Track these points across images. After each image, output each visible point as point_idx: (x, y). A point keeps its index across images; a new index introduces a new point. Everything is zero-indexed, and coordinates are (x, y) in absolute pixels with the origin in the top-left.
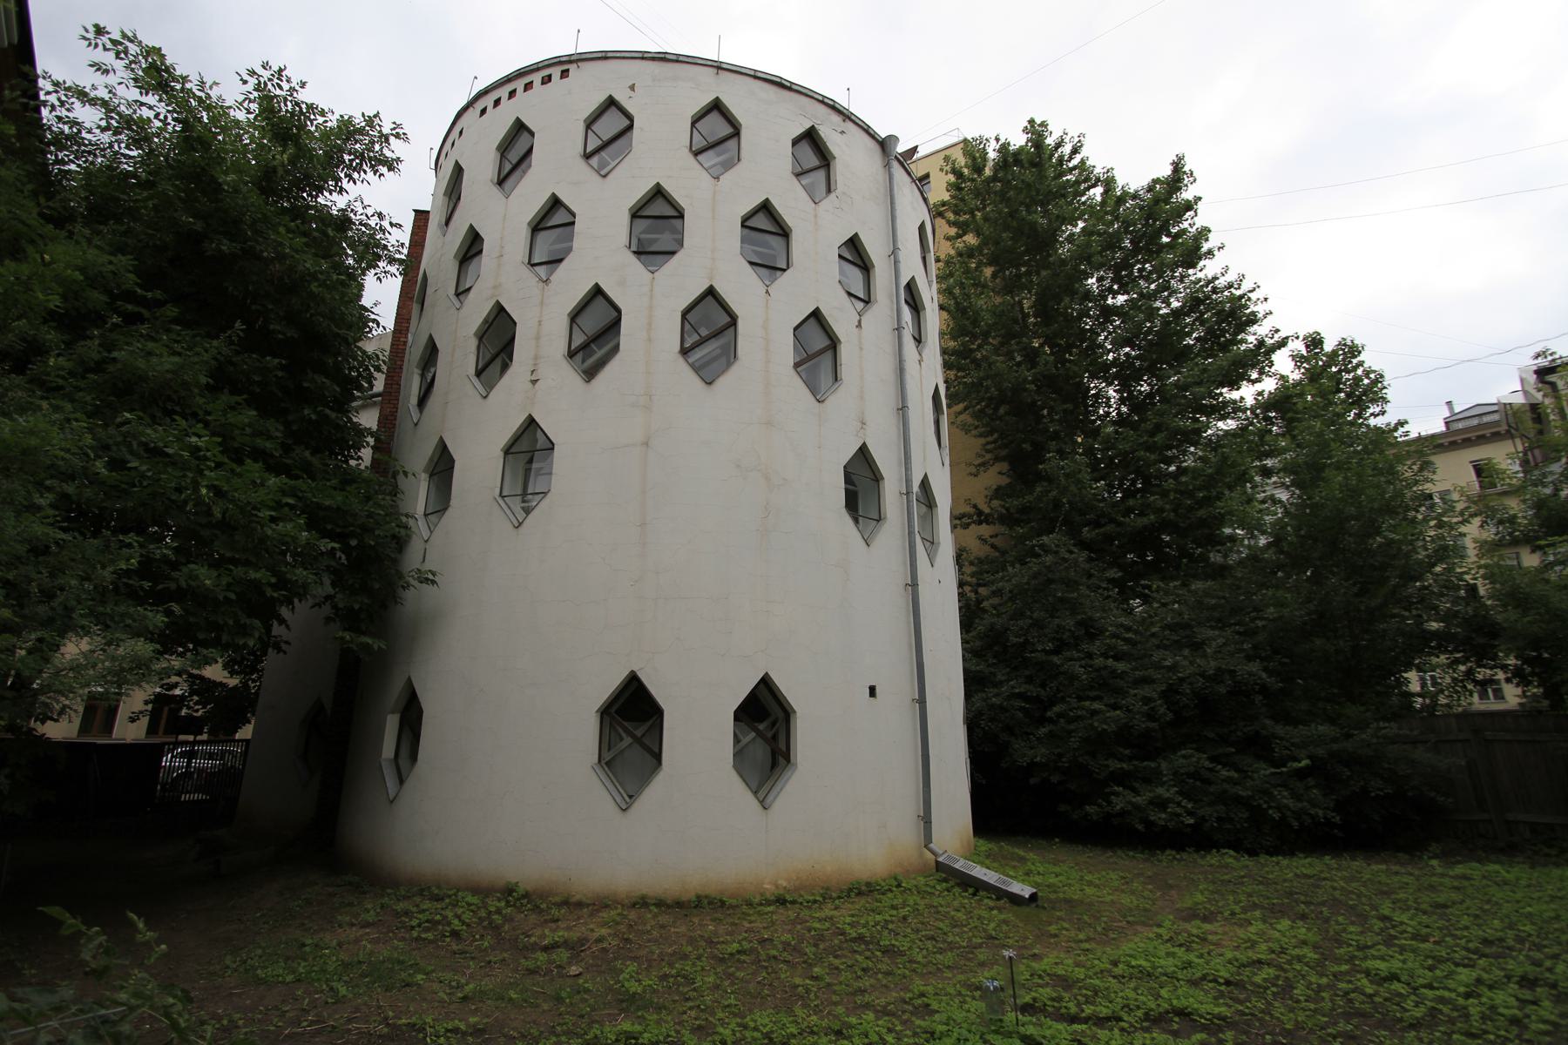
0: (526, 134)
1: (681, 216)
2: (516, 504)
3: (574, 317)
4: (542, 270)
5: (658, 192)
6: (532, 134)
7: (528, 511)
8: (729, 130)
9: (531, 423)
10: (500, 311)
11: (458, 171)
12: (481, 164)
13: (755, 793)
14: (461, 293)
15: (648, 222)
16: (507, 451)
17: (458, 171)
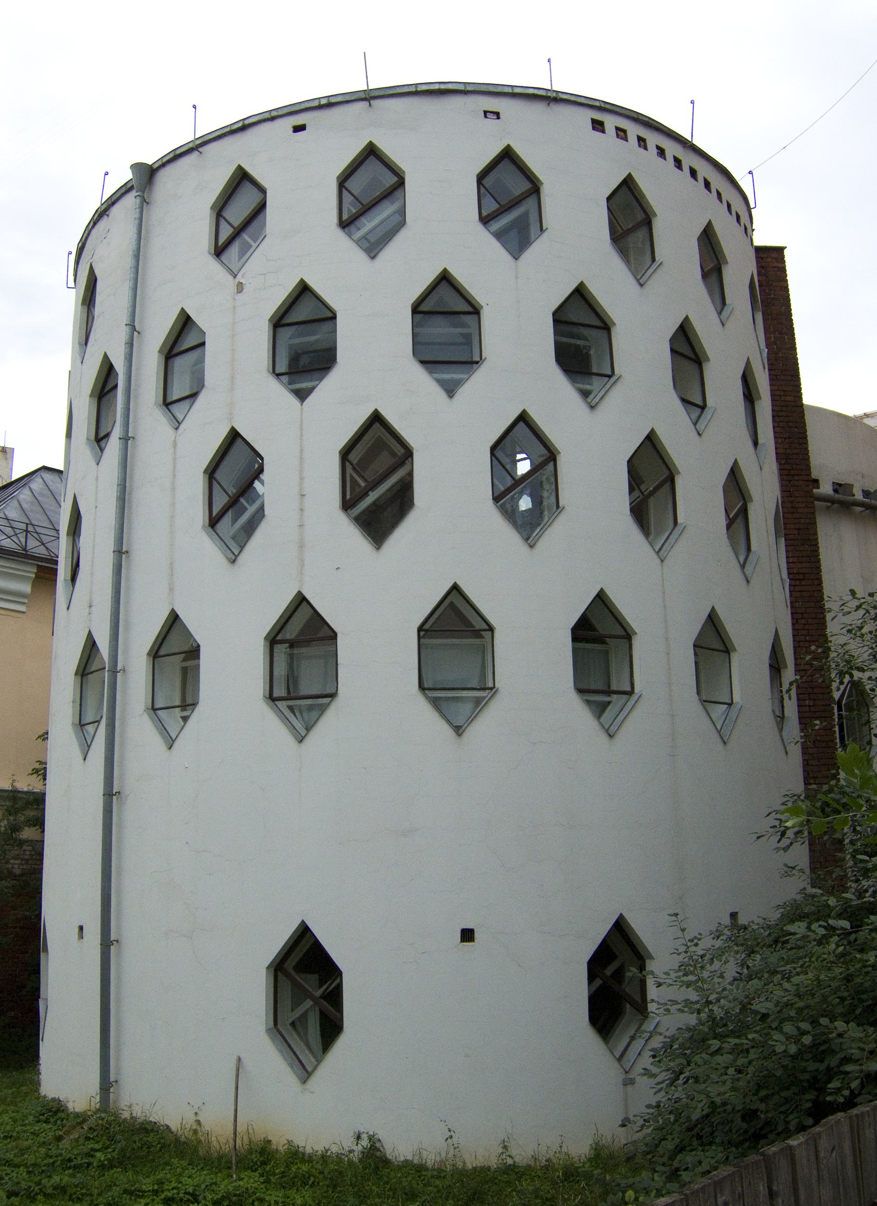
1: (334, 317)
3: (211, 472)
5: (303, 290)
9: (174, 619)
15: (293, 329)
16: (156, 654)
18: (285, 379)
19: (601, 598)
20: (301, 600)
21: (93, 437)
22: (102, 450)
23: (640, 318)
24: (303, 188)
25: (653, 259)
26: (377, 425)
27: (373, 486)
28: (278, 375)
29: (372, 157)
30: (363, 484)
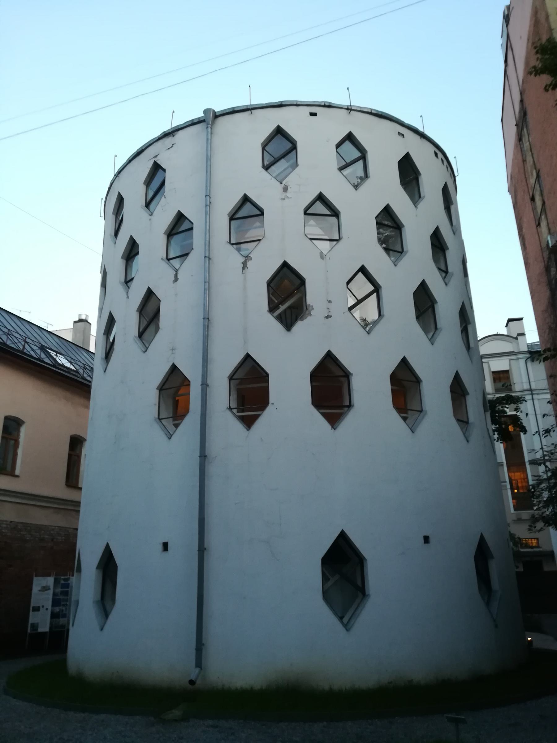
0: (160, 170)
1: (262, 214)
2: (169, 424)
4: (176, 263)
5: (246, 199)
6: (164, 170)
7: (177, 426)
8: (290, 145)
10: (150, 293)
11: (120, 200)
12: (135, 196)
13: (341, 618)
14: (128, 281)
17: (120, 200)
18: (235, 246)
19: (404, 361)
20: (248, 357)
21: (123, 280)
22: (129, 288)
23: (417, 224)
24: (245, 142)
25: (420, 197)
26: (285, 269)
27: (282, 302)
28: (232, 244)
29: (279, 135)
30: (276, 301)
